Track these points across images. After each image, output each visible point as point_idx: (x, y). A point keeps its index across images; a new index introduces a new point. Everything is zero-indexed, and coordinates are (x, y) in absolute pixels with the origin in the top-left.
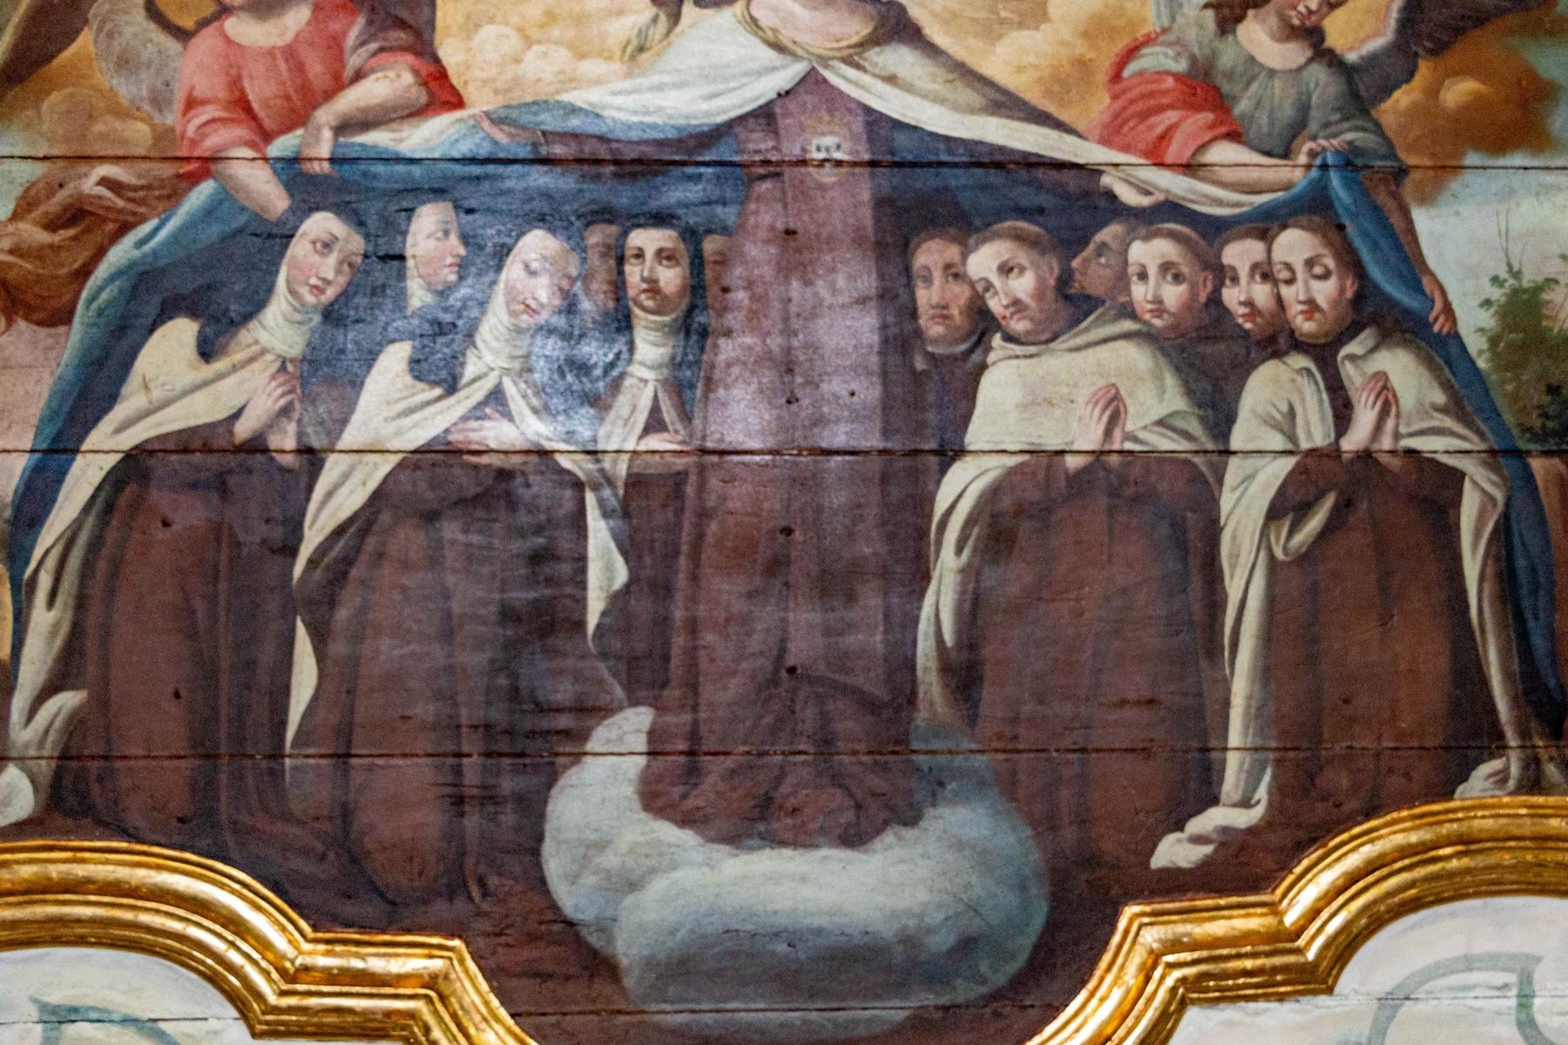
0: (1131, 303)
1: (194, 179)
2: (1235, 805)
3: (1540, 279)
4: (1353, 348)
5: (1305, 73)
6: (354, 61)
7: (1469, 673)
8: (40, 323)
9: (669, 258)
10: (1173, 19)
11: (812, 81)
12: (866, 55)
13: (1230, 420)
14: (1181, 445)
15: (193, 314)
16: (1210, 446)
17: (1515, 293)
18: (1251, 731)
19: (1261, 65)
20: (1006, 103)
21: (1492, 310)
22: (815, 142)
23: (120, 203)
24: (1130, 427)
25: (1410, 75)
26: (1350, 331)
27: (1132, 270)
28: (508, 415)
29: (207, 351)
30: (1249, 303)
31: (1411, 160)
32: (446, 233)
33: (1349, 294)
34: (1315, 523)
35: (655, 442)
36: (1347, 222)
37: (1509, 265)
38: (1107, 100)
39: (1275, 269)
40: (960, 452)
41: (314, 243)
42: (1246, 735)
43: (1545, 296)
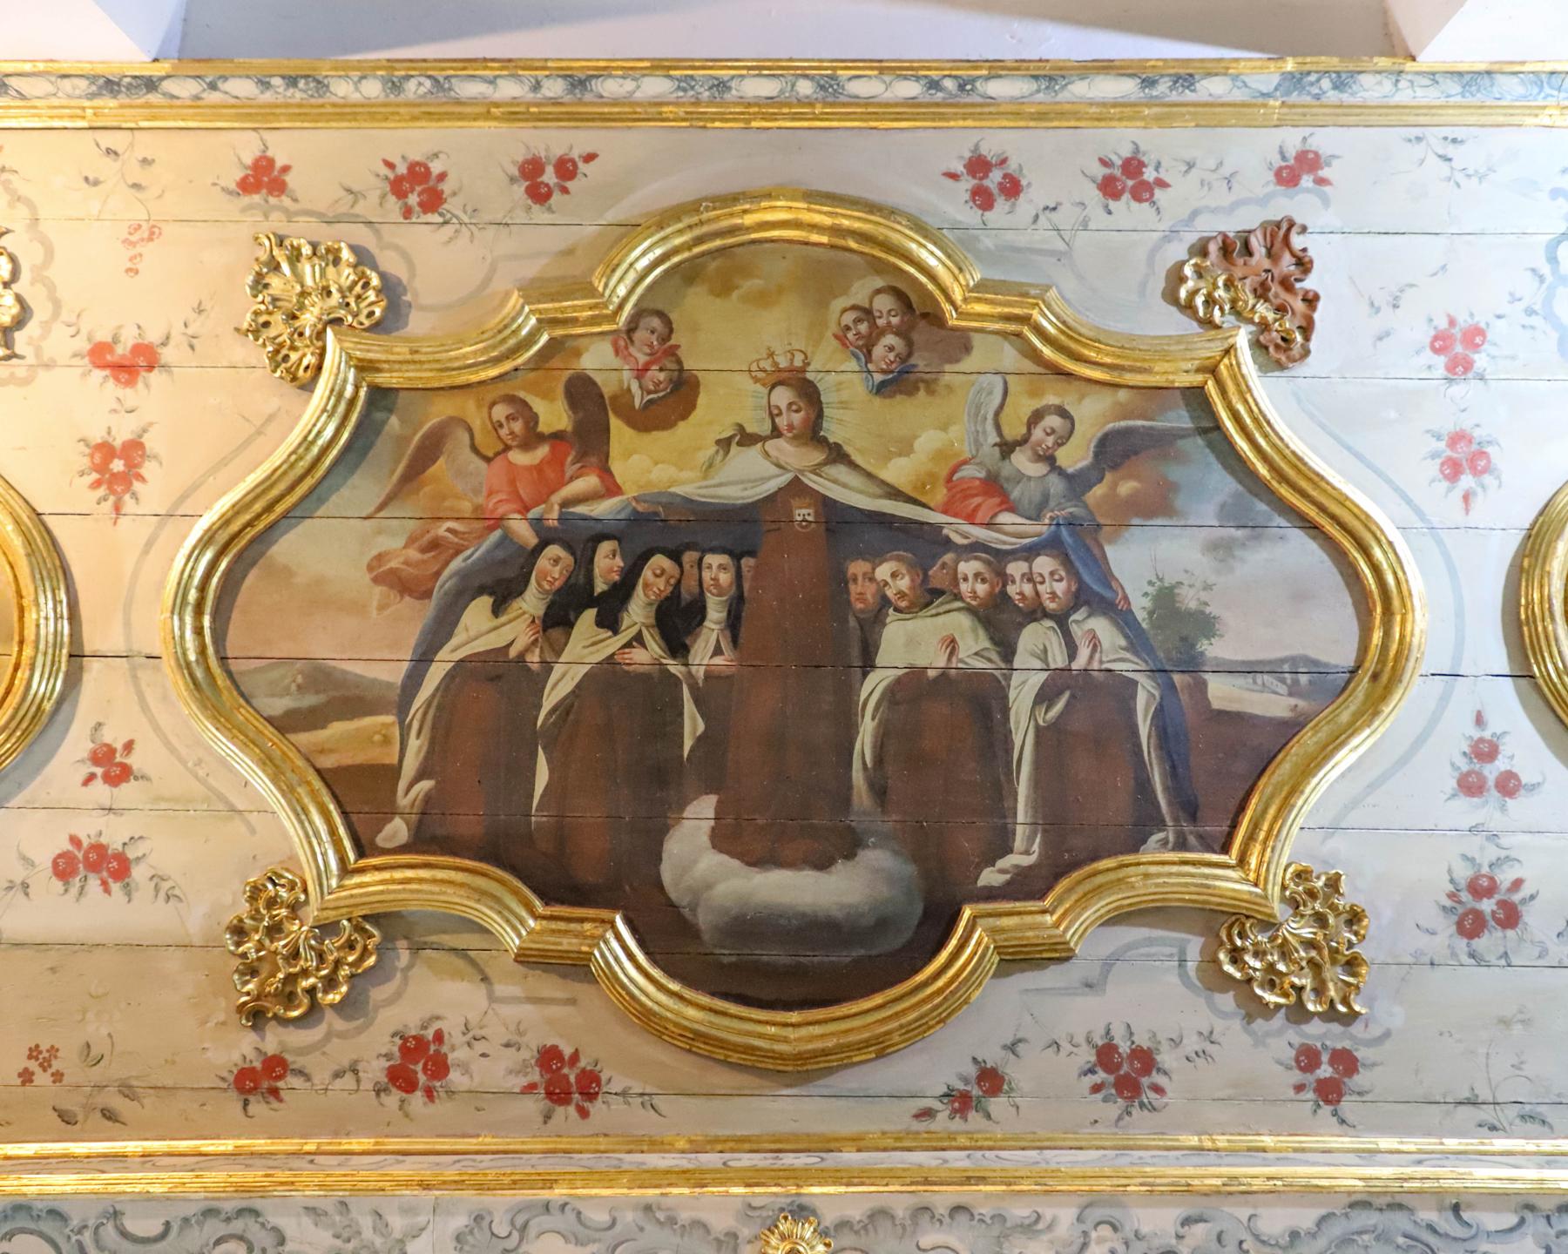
1: (491, 529)
4: (1076, 617)
6: (569, 473)
7: (1143, 786)
10: (977, 451)
11: (796, 482)
13: (1014, 653)
14: (988, 665)
16: (1003, 666)
17: (1161, 589)
22: (797, 512)
23: (456, 540)
25: (1100, 480)
27: (960, 576)
30: (1021, 593)
34: (1059, 706)
35: (718, 660)
40: (873, 667)
43: (1176, 591)
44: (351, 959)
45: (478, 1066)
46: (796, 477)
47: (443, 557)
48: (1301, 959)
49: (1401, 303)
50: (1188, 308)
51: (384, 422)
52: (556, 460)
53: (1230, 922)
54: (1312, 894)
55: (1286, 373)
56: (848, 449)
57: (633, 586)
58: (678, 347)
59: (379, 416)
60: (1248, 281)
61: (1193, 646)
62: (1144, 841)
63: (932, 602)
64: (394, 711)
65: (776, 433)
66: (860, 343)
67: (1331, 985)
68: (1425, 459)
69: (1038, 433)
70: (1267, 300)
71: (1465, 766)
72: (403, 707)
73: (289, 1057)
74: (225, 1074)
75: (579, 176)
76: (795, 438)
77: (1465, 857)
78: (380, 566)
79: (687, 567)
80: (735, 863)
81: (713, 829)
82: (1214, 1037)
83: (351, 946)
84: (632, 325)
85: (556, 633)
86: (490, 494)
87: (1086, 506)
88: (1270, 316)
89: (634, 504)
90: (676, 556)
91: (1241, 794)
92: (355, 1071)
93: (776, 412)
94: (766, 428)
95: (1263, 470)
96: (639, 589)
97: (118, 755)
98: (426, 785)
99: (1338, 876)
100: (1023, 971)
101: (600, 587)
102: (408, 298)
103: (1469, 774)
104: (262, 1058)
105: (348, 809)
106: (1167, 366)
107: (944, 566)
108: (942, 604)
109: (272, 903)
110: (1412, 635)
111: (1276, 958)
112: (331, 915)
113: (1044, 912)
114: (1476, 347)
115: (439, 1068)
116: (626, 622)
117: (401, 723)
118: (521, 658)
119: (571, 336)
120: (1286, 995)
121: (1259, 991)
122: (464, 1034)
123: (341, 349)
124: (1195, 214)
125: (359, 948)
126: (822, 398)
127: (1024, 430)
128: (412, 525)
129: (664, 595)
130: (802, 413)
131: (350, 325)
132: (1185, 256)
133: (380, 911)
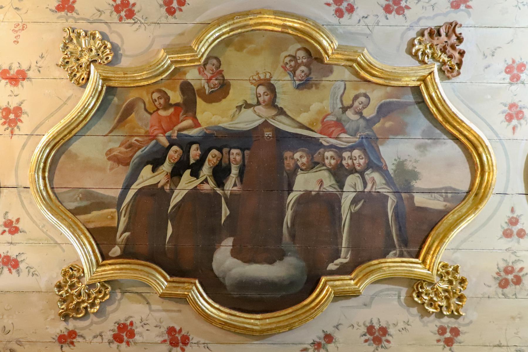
0: (325, 163)
2: (343, 258)
3: (404, 160)
5: (359, 121)
6: (181, 118)
7: (389, 234)
8: (123, 166)
9: (238, 155)
10: (333, 111)
12: (276, 117)
13: (344, 185)
14: (335, 190)
15: (151, 164)
17: (399, 162)
18: (347, 244)
19: (350, 119)
20: (302, 126)
21: (394, 165)
22: (266, 133)
23: (139, 144)
24: (324, 187)
25: (379, 121)
26: (367, 169)
27: (325, 157)
28: (207, 183)
29: (154, 170)
30: (347, 164)
31: (379, 137)
32: (197, 150)
33: (367, 162)
35: (235, 188)
36: (366, 148)
37: (398, 157)
38: (321, 125)
39: (353, 157)
41: (173, 151)
42: (346, 245)
43: (405, 163)
44: (100, 296)
45: (145, 334)
46: (266, 120)
47: (134, 150)
48: (443, 296)
49: (495, 54)
50: (415, 56)
51: (112, 99)
52: (176, 114)
53: (418, 283)
54: (448, 273)
55: (450, 81)
56: (285, 109)
57: (204, 161)
58: (223, 71)
59: (110, 97)
60: (438, 46)
61: (410, 183)
62: (388, 254)
63: (314, 167)
64: (116, 207)
65: (259, 103)
66: (291, 69)
67: (452, 305)
68: (500, 113)
69: (356, 104)
70: (445, 53)
71: (506, 227)
72: (119, 205)
73: (77, 331)
74: (54, 337)
75: (186, 4)
76: (266, 105)
77: (503, 260)
78: (110, 154)
79: (224, 154)
80: (239, 262)
81: (232, 250)
82: (409, 323)
83: (100, 292)
84: (206, 63)
85: (175, 178)
86: (151, 127)
87: (372, 131)
88: (446, 59)
89: (205, 130)
90: (220, 150)
91: (424, 237)
92: (101, 336)
93: (259, 95)
94: (255, 102)
95: (440, 118)
96: (206, 162)
97: (14, 223)
98: (127, 234)
99: (458, 267)
100: (342, 300)
101: (192, 161)
102: (121, 52)
103: (507, 230)
104: (68, 331)
105: (98, 243)
106: (407, 79)
107: (319, 153)
108: (318, 168)
109: (71, 277)
110: (492, 180)
111: (433, 295)
112: (93, 281)
113: (351, 279)
114: (522, 71)
115: (132, 334)
116: (201, 175)
117: (118, 211)
118: (163, 187)
119: (183, 67)
120: (436, 309)
121: (427, 308)
122: (141, 323)
123: (97, 72)
124: (420, 19)
125: (103, 292)
126: (277, 91)
127: (351, 102)
128: (122, 138)
129: (215, 164)
130: (269, 96)
131: (100, 63)
132: (415, 36)
133: (111, 279)
